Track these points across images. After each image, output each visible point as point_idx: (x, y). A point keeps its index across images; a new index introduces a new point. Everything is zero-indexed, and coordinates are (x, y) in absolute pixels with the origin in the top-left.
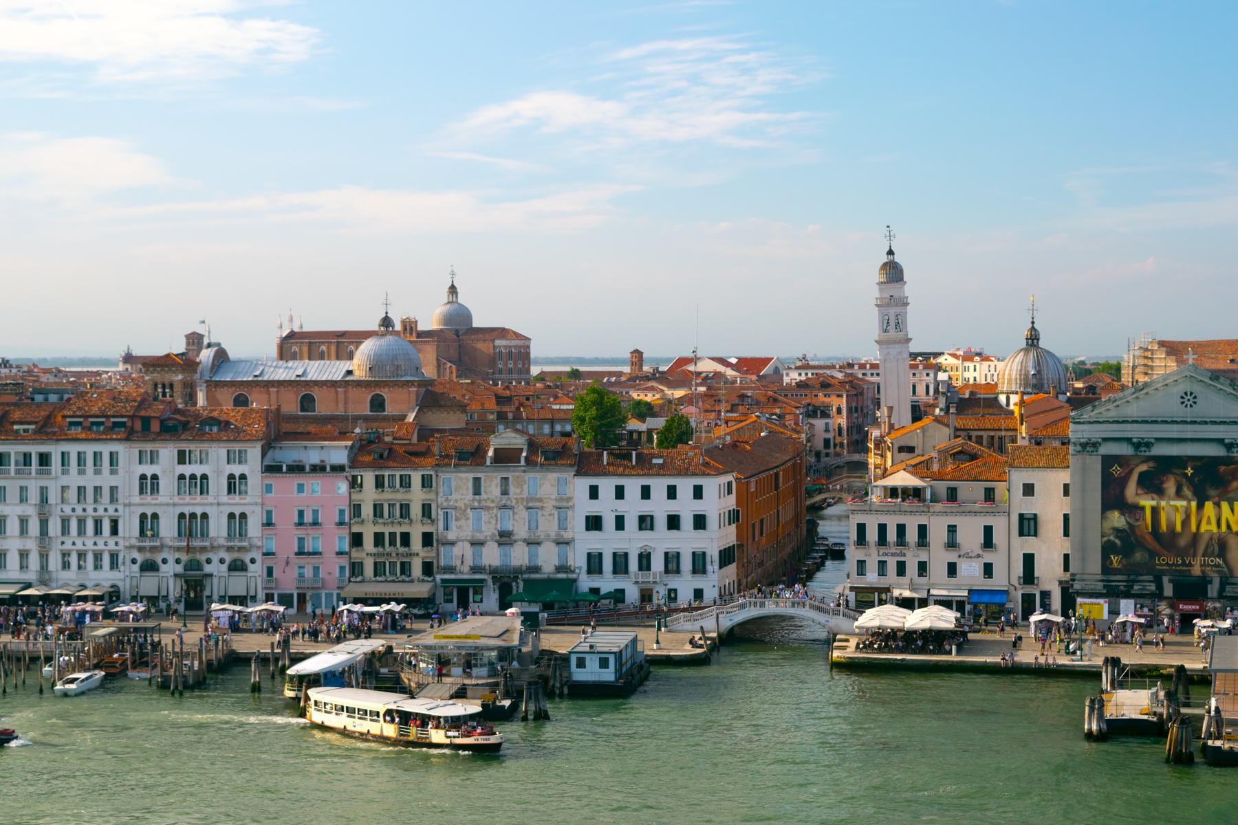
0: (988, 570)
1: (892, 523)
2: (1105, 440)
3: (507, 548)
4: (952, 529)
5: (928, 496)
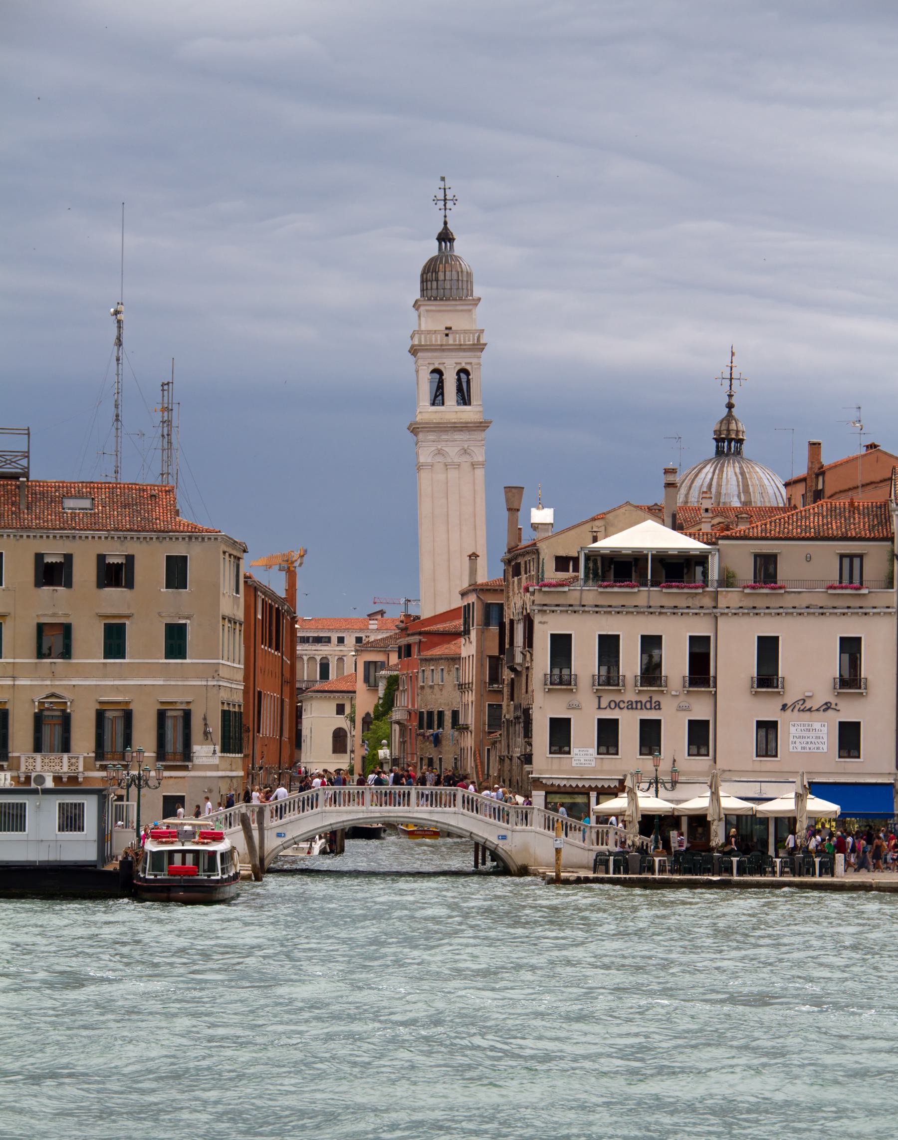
1: (630, 633)
4: (768, 648)
5: (714, 574)
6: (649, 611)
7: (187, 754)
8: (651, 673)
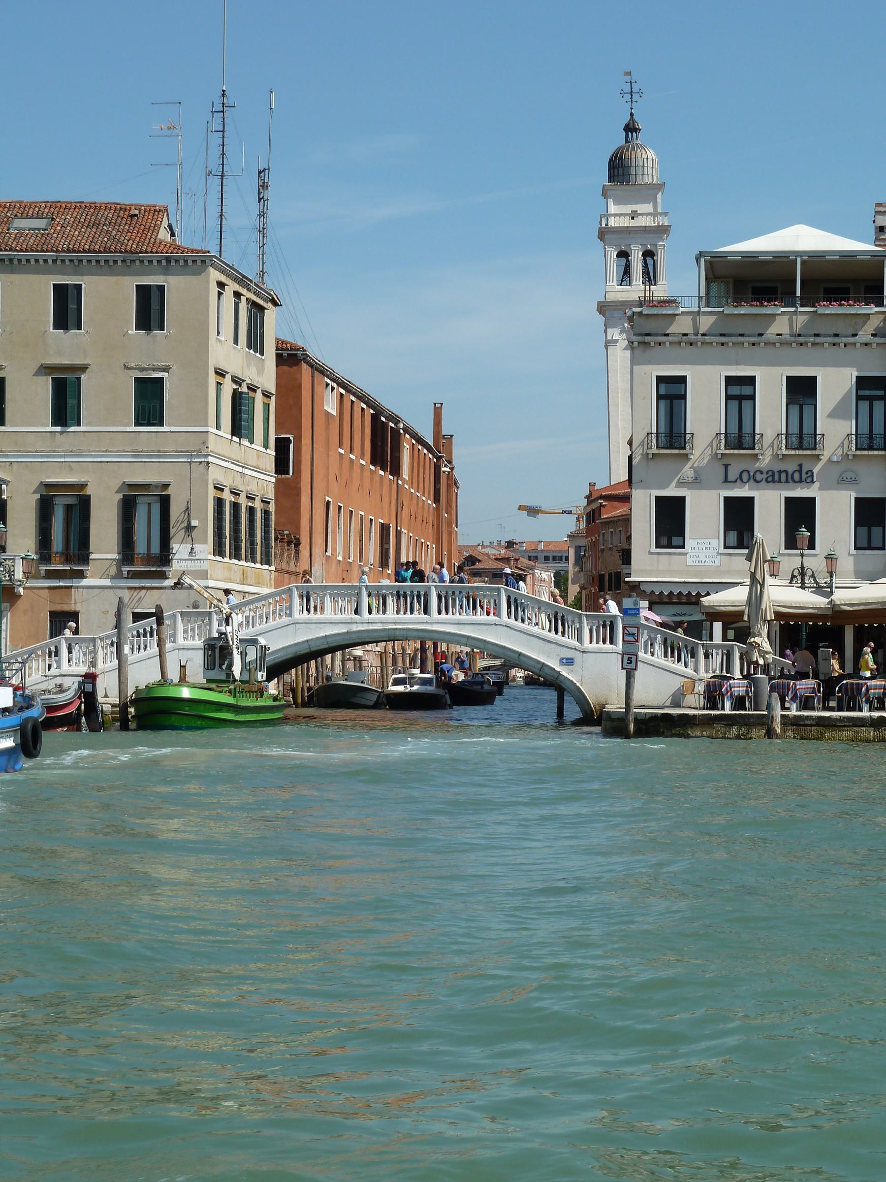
6: (798, 339)
7: (165, 557)
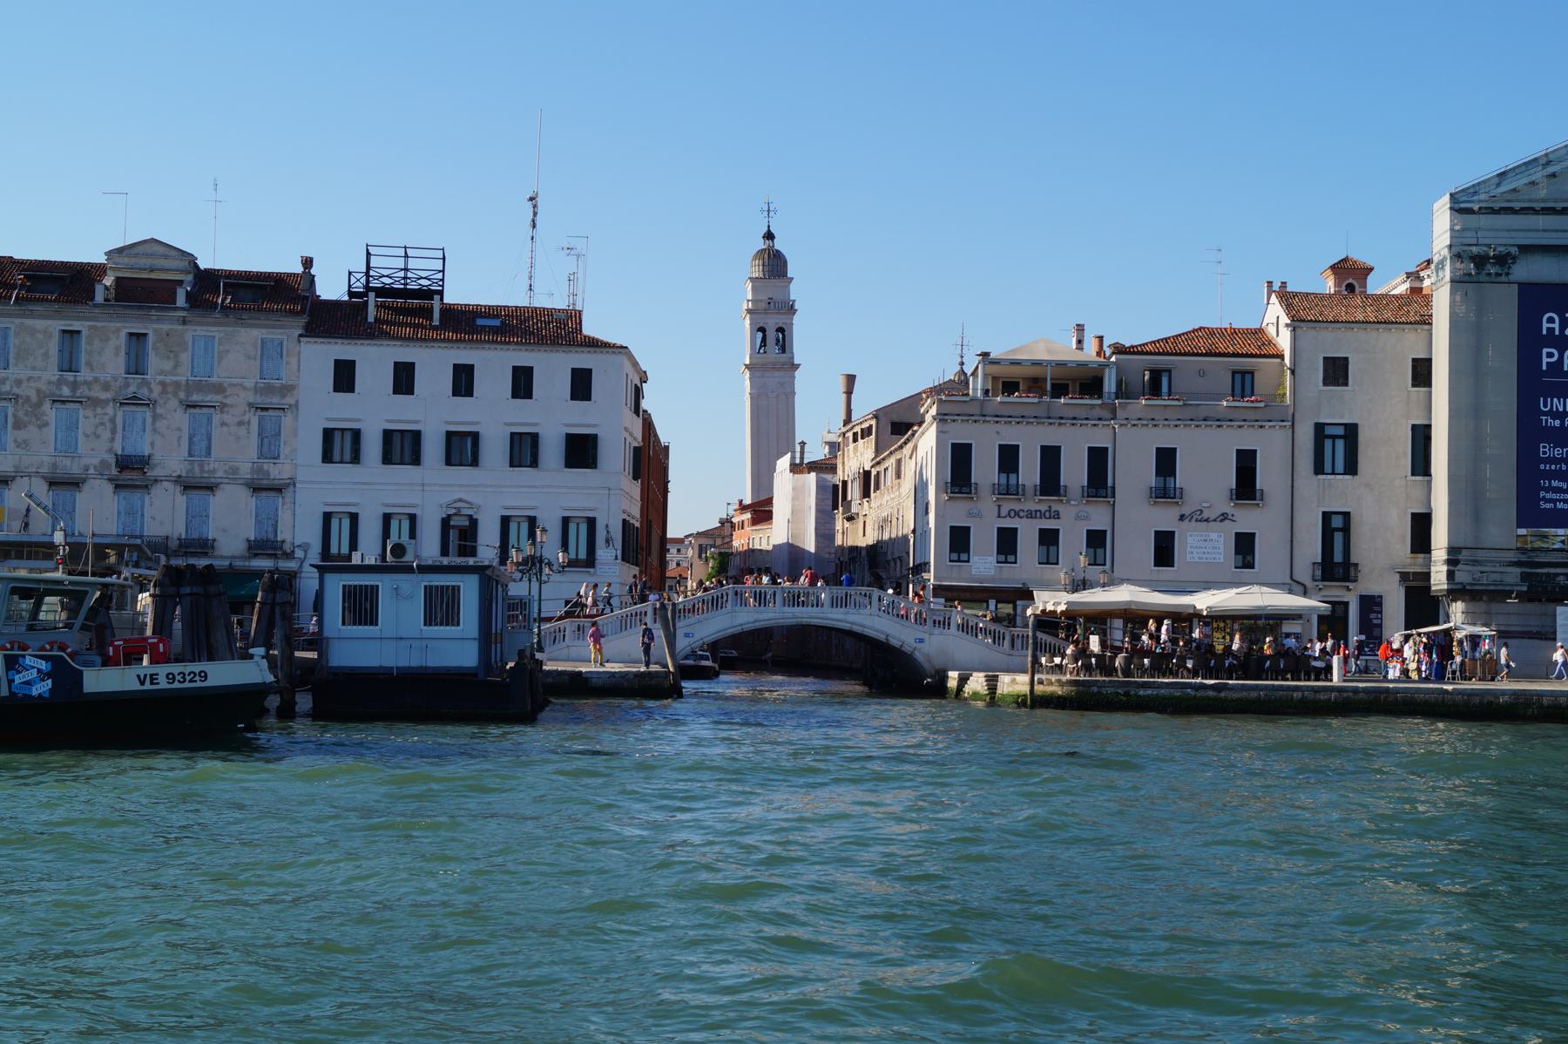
0: (1245, 546)
2: (1526, 249)
3: (136, 496)
4: (1166, 461)
5: (1109, 385)
7: (590, 561)
8: (1050, 483)
